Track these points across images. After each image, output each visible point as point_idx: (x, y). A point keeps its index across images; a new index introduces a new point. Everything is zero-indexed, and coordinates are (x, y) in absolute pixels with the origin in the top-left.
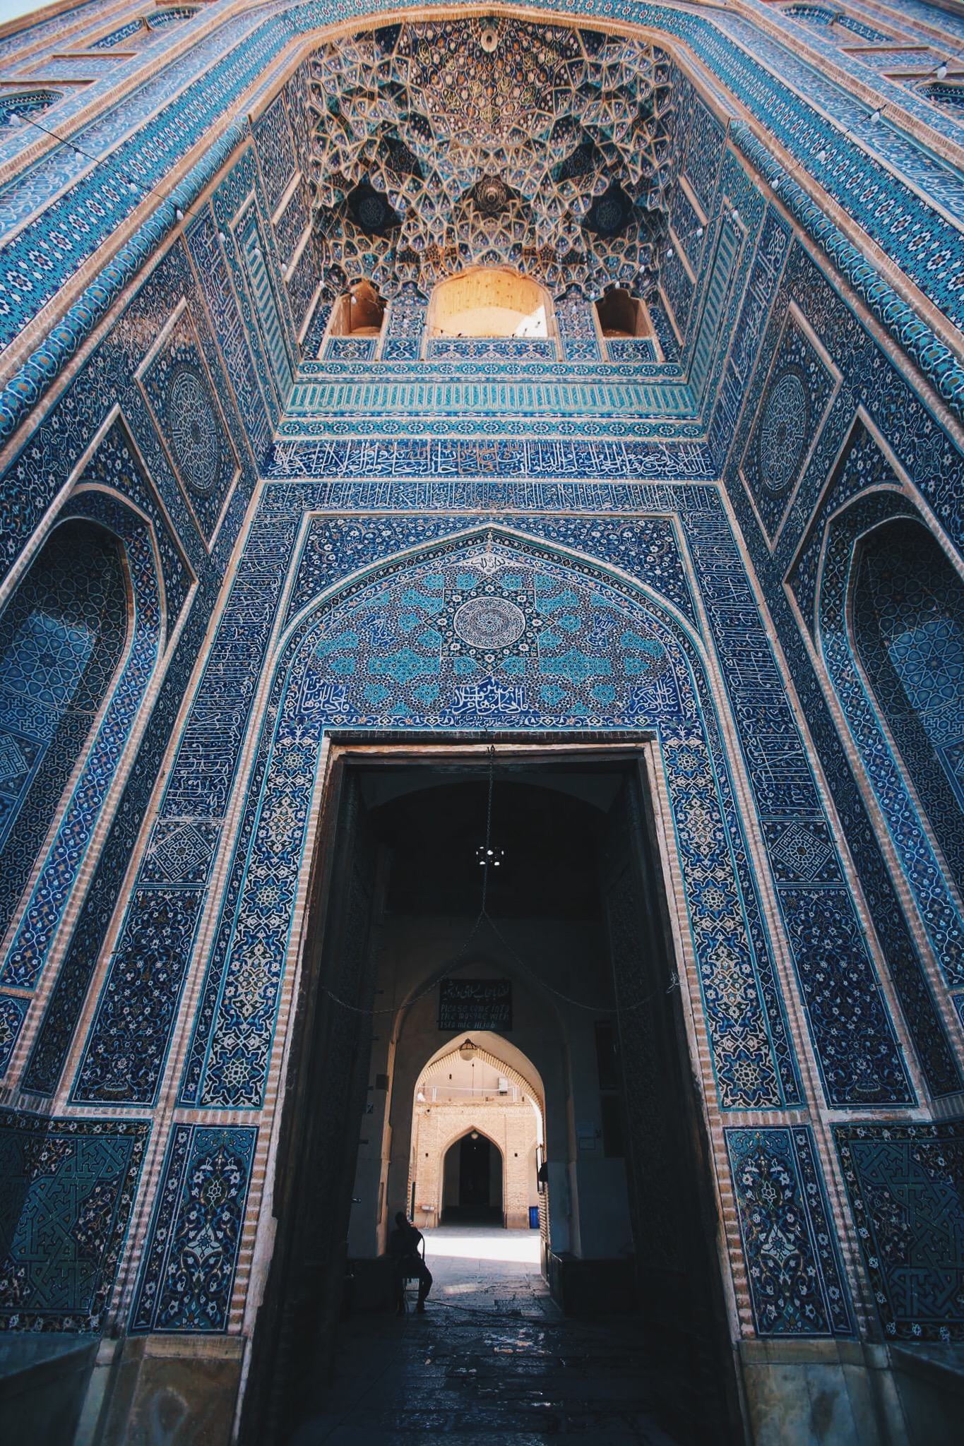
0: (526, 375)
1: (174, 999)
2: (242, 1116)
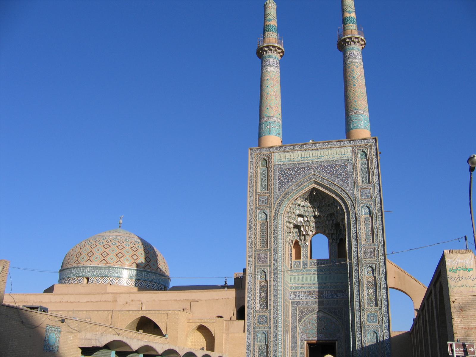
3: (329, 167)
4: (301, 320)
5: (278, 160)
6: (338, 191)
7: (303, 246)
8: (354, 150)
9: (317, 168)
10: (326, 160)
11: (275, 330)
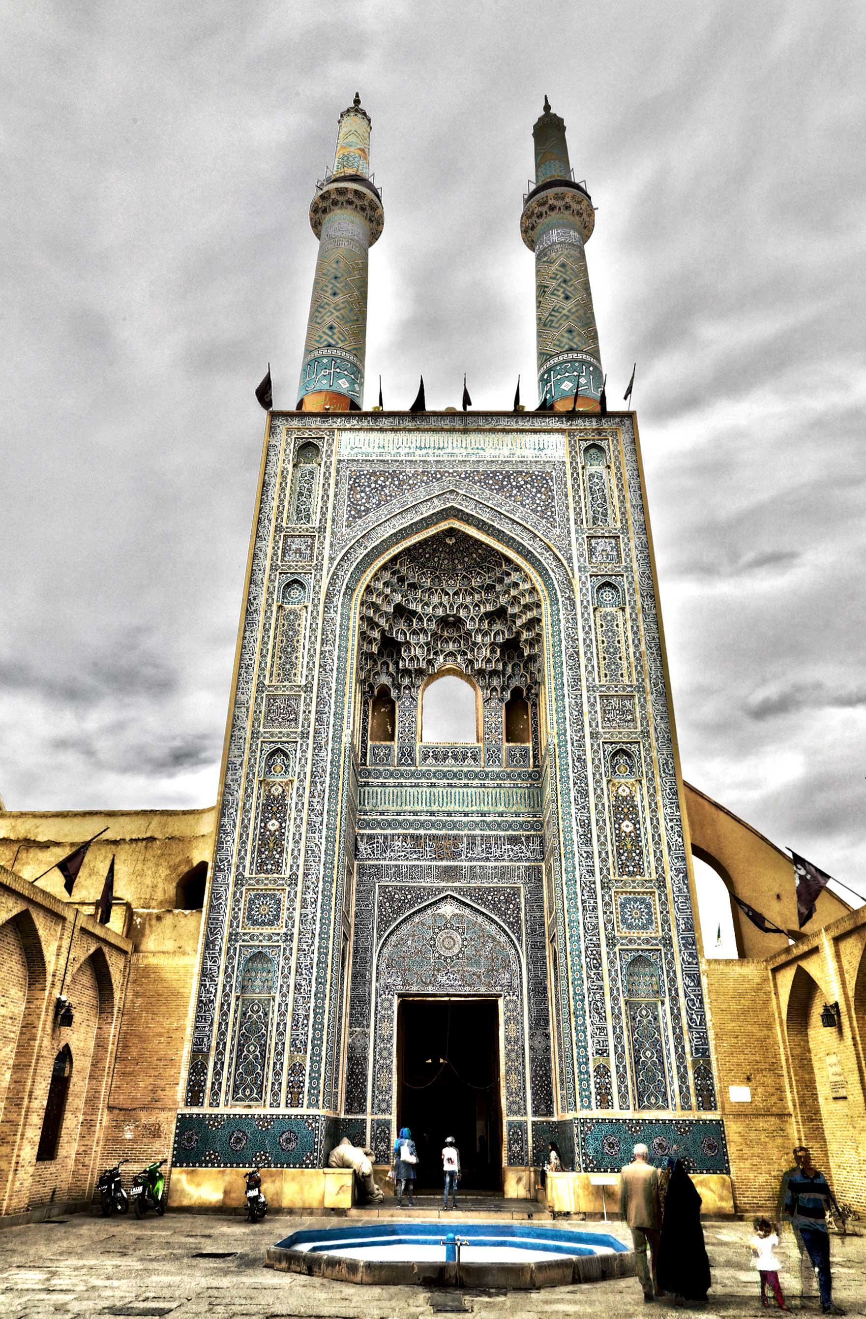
0: (466, 781)
1: (366, 1086)
2: (387, 1117)
3: (501, 479)
4: (388, 923)
5: (352, 449)
6: (522, 538)
7: (403, 703)
8: (570, 441)
9: (463, 476)
10: (490, 459)
11: (305, 946)
